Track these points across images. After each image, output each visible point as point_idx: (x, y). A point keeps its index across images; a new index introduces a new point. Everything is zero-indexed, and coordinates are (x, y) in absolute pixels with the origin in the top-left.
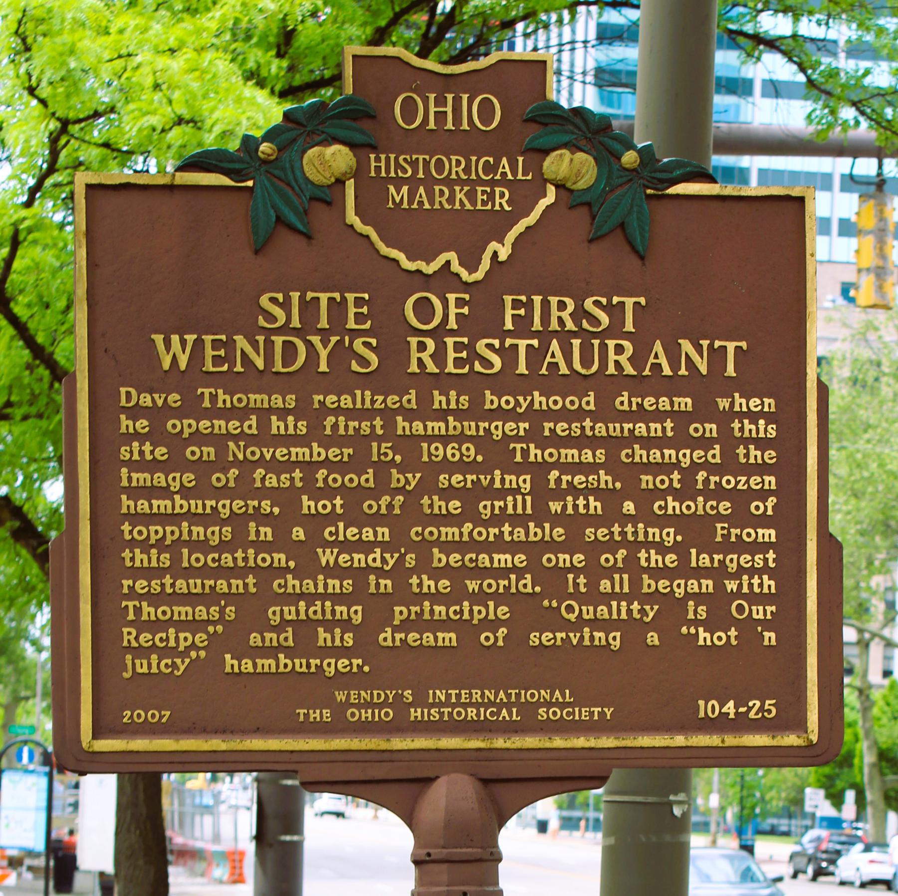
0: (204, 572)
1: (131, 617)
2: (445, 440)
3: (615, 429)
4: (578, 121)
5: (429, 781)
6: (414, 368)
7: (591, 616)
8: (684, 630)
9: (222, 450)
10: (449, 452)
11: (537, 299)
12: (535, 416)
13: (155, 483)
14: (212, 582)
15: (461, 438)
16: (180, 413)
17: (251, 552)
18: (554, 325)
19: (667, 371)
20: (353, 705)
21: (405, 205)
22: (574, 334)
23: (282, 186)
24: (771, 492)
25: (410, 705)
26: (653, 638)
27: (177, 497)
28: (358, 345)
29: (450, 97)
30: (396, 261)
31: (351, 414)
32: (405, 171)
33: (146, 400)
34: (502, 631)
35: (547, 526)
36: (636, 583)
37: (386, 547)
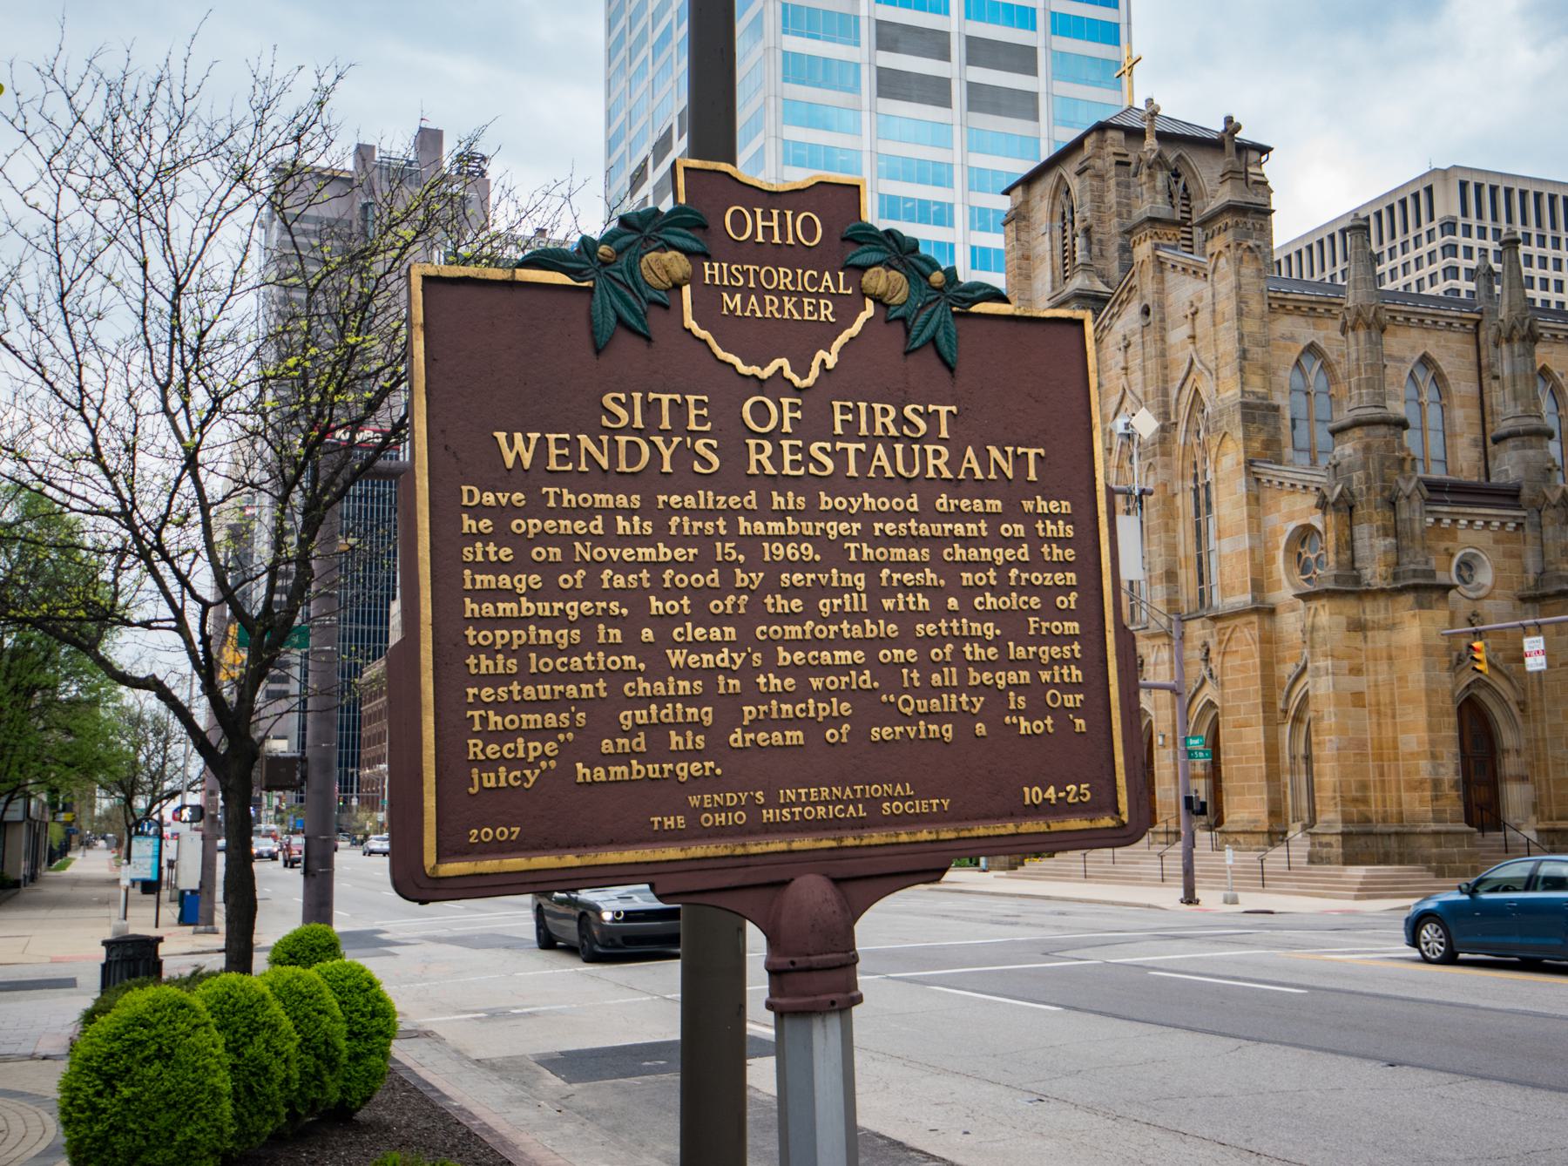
0: (554, 677)
1: (477, 727)
2: (785, 539)
3: (937, 529)
4: (891, 242)
5: (784, 884)
6: (753, 469)
7: (925, 710)
8: (1007, 719)
9: (568, 550)
10: (789, 551)
11: (863, 405)
12: (867, 517)
13: (500, 585)
14: (561, 688)
15: (800, 538)
16: (525, 513)
17: (601, 654)
18: (879, 431)
19: (979, 475)
20: (706, 810)
21: (739, 313)
22: (896, 439)
23: (621, 289)
24: (1072, 588)
25: (762, 806)
26: (980, 728)
27: (523, 599)
28: (699, 445)
29: (775, 212)
30: (733, 366)
31: (695, 514)
32: (737, 280)
33: (489, 498)
34: (846, 727)
35: (881, 622)
36: (963, 676)
37: (732, 646)
